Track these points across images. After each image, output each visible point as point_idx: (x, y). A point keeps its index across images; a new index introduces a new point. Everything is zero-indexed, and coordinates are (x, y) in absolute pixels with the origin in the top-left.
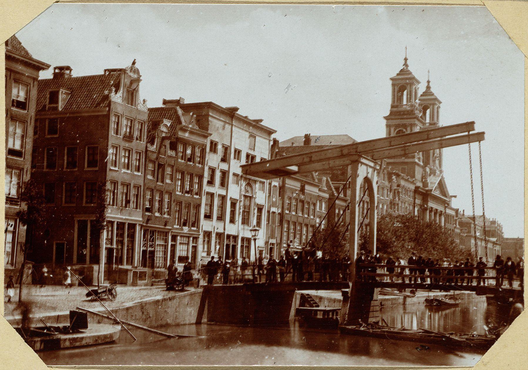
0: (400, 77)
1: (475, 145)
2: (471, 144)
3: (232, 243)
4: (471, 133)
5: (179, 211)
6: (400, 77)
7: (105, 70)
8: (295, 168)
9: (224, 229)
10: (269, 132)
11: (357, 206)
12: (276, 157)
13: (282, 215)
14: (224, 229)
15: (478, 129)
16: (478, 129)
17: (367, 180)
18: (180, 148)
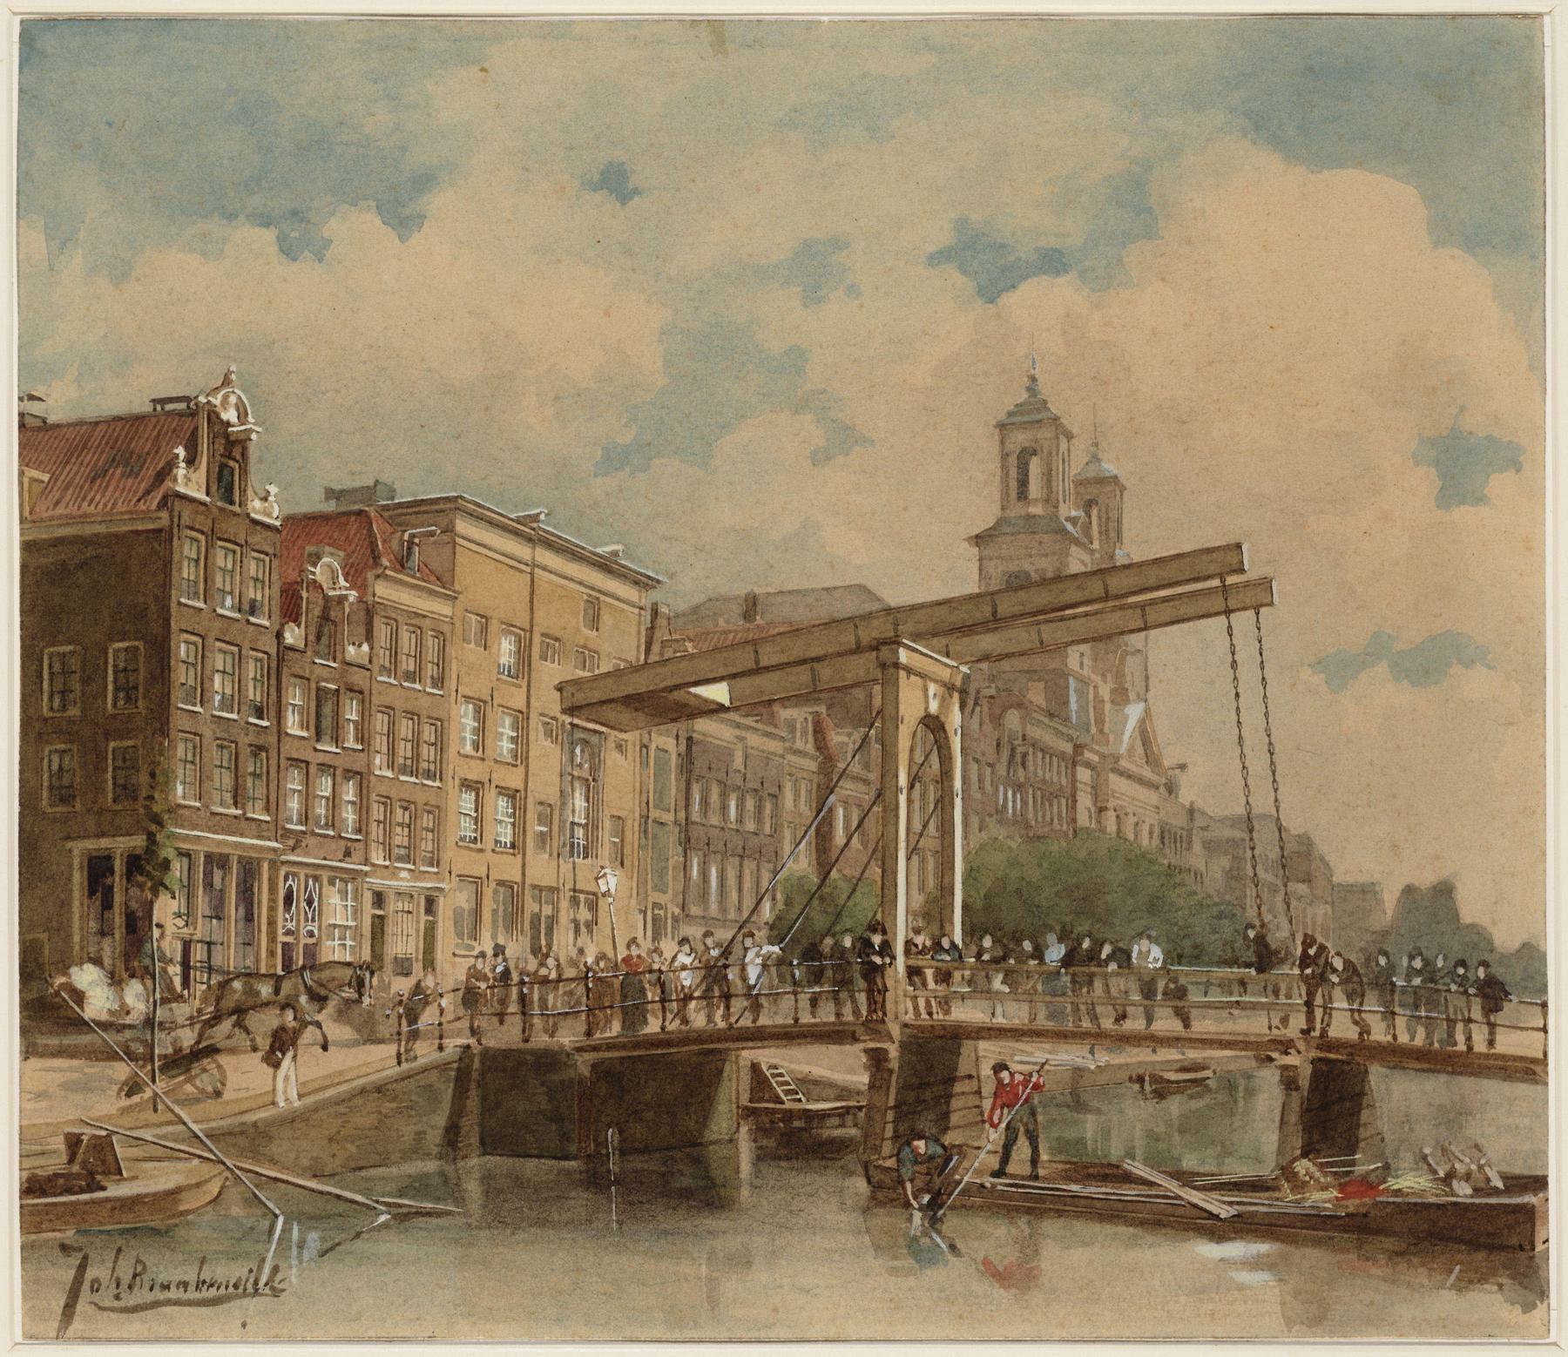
0: (1018, 419)
1: (1243, 620)
2: (1232, 616)
3: (547, 910)
4: (1231, 580)
5: (384, 822)
6: (1018, 419)
7: (154, 401)
8: (718, 693)
9: (524, 874)
10: (644, 583)
11: (903, 798)
12: (662, 654)
13: (686, 826)
14: (524, 874)
15: (1253, 571)
16: (1253, 571)
17: (933, 725)
18: (382, 632)
